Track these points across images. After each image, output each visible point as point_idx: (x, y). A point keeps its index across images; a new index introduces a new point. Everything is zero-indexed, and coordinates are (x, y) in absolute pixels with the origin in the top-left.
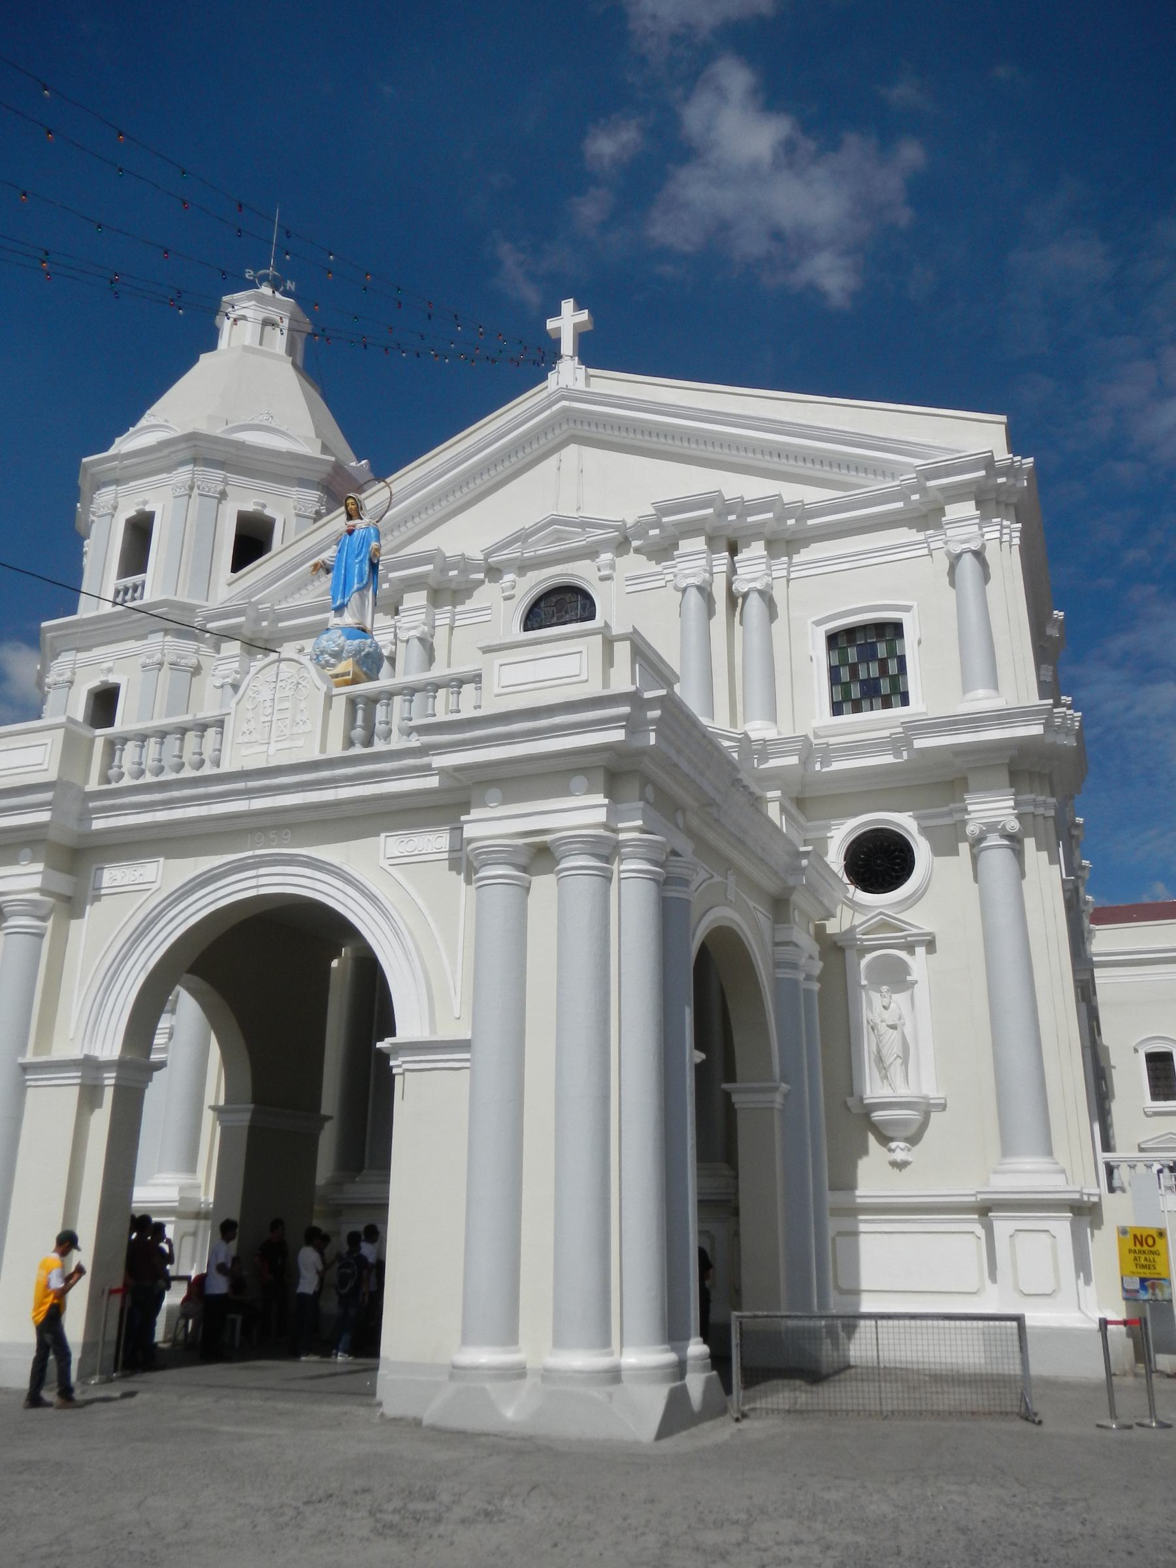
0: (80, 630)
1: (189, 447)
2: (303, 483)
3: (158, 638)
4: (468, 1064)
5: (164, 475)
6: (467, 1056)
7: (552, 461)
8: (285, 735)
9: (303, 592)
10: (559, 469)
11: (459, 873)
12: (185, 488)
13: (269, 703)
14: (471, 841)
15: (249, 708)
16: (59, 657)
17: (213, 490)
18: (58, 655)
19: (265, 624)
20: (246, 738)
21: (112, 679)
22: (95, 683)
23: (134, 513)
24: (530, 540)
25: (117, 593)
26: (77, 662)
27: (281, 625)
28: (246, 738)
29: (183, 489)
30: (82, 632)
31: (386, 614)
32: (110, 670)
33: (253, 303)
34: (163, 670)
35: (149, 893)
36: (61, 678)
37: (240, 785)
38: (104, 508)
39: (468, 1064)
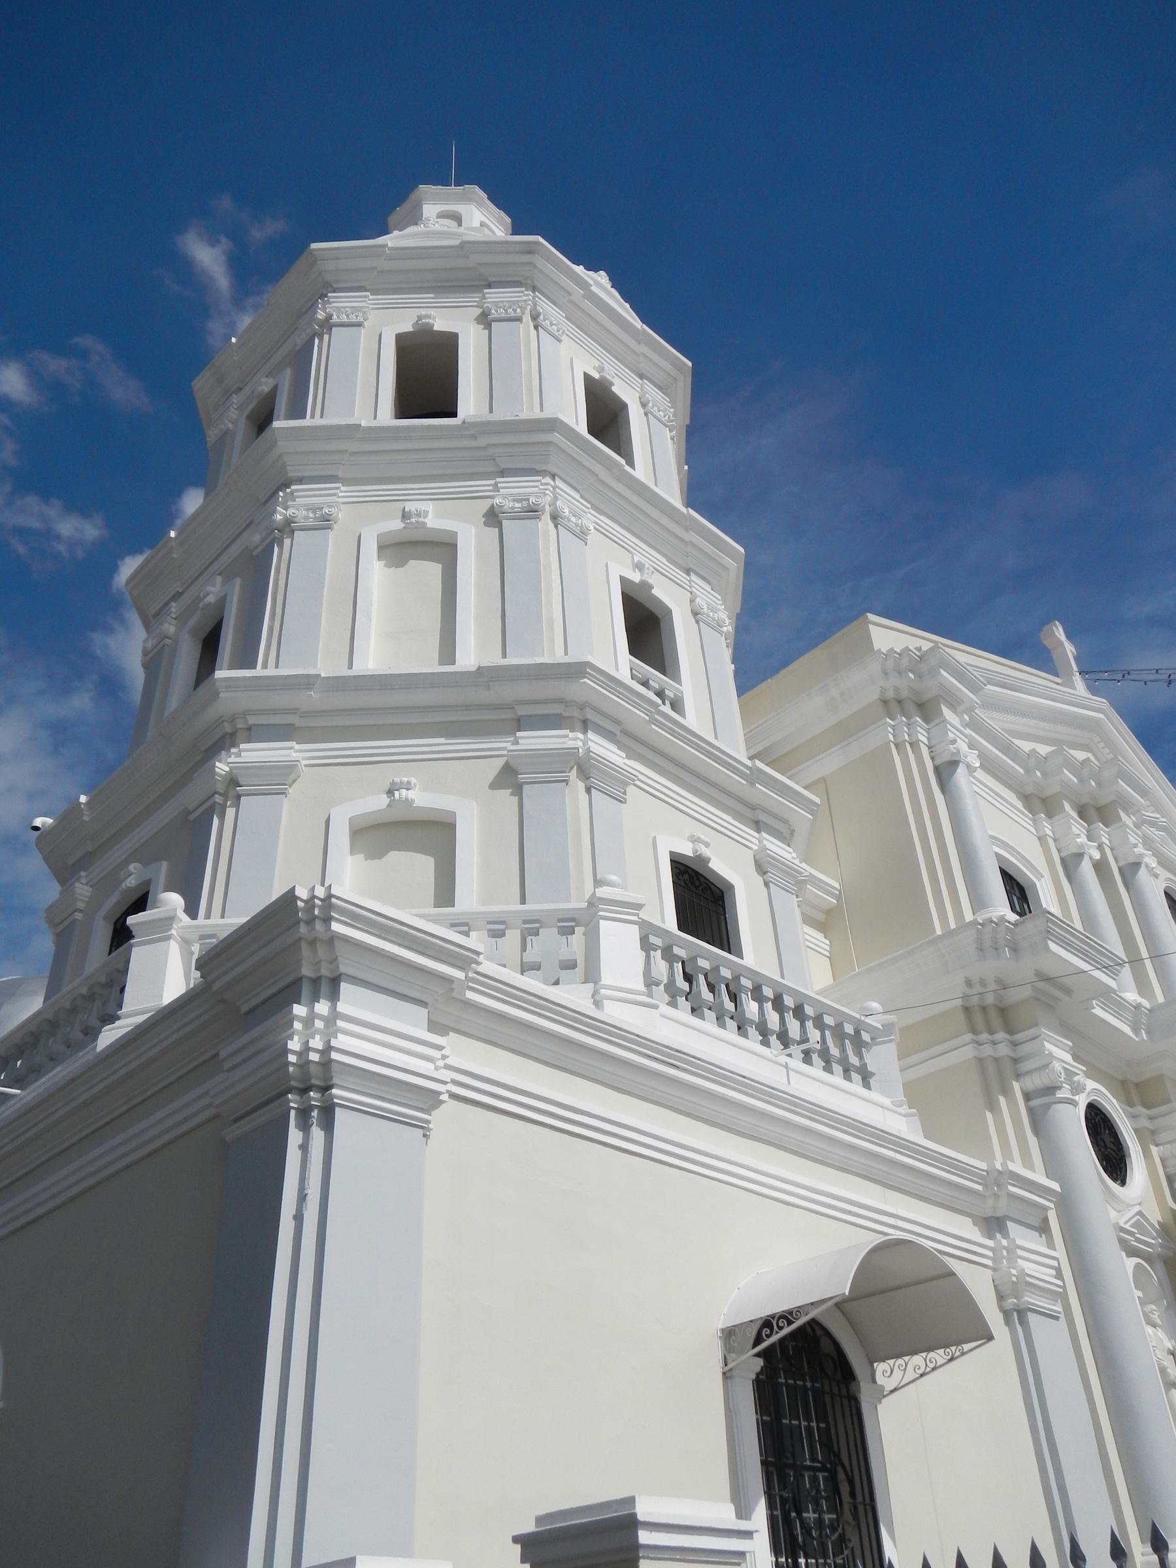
38: (551, 324)
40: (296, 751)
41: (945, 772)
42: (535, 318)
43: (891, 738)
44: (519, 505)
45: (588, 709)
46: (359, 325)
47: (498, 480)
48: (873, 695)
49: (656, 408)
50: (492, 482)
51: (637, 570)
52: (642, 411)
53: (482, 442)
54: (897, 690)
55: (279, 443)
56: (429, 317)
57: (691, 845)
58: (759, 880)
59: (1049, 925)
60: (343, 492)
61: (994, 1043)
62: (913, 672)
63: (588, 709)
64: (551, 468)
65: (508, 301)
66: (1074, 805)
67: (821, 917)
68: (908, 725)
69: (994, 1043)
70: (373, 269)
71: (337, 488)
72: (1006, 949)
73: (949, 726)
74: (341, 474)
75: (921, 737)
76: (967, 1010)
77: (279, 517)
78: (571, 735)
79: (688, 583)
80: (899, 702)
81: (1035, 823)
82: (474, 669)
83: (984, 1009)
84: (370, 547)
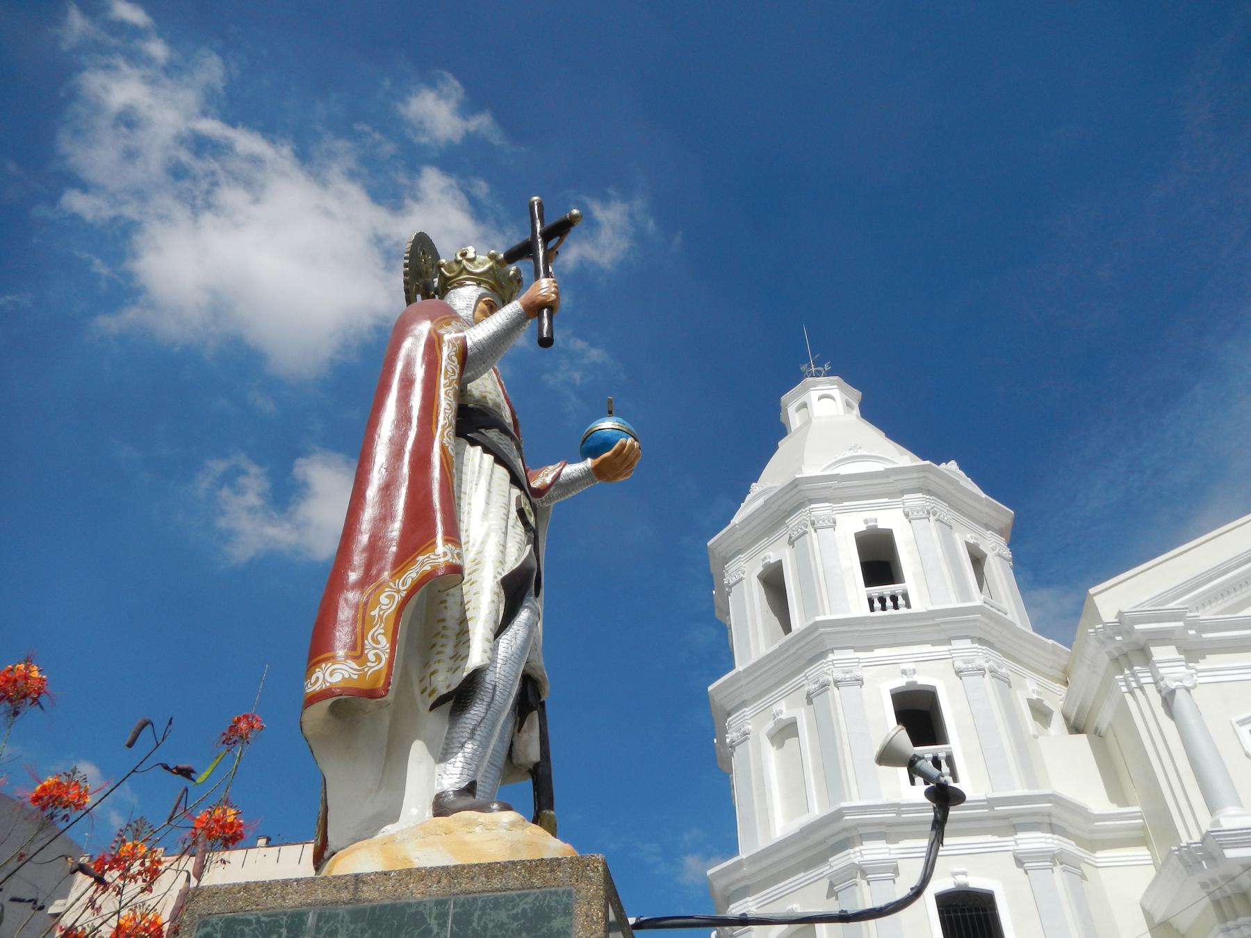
0: (861, 628)
1: (918, 478)
2: (987, 527)
3: (967, 643)
5: (886, 500)
9: (1208, 608)
12: (924, 512)
16: (830, 655)
17: (946, 518)
18: (832, 650)
19: (1192, 632)
21: (923, 680)
22: (900, 682)
23: (865, 529)
25: (871, 602)
26: (861, 661)
27: (1204, 636)
29: (921, 513)
30: (862, 631)
32: (914, 672)
33: (836, 387)
34: (985, 676)
36: (848, 676)
38: (824, 521)
40: (750, 902)
41: (1168, 699)
42: (813, 524)
43: (1124, 689)
44: (816, 686)
45: (859, 828)
46: (741, 579)
47: (806, 671)
48: (1106, 659)
49: (915, 513)
50: (803, 674)
51: (904, 676)
52: (907, 520)
53: (792, 651)
54: (1117, 649)
55: (715, 698)
56: (765, 558)
57: (953, 879)
58: (1022, 870)
59: (1217, 839)
60: (747, 711)
61: (1238, 927)
62: (1119, 634)
63: (859, 828)
64: (828, 647)
65: (797, 524)
67: (1140, 833)
68: (1133, 674)
69: (1238, 927)
70: (737, 539)
71: (745, 711)
72: (1203, 862)
73: (1158, 665)
74: (746, 697)
75: (1143, 680)
76: (1217, 903)
77: (728, 740)
78: (851, 851)
79: (948, 653)
80: (1125, 655)
82: (798, 830)
83: (1229, 897)
84: (766, 742)
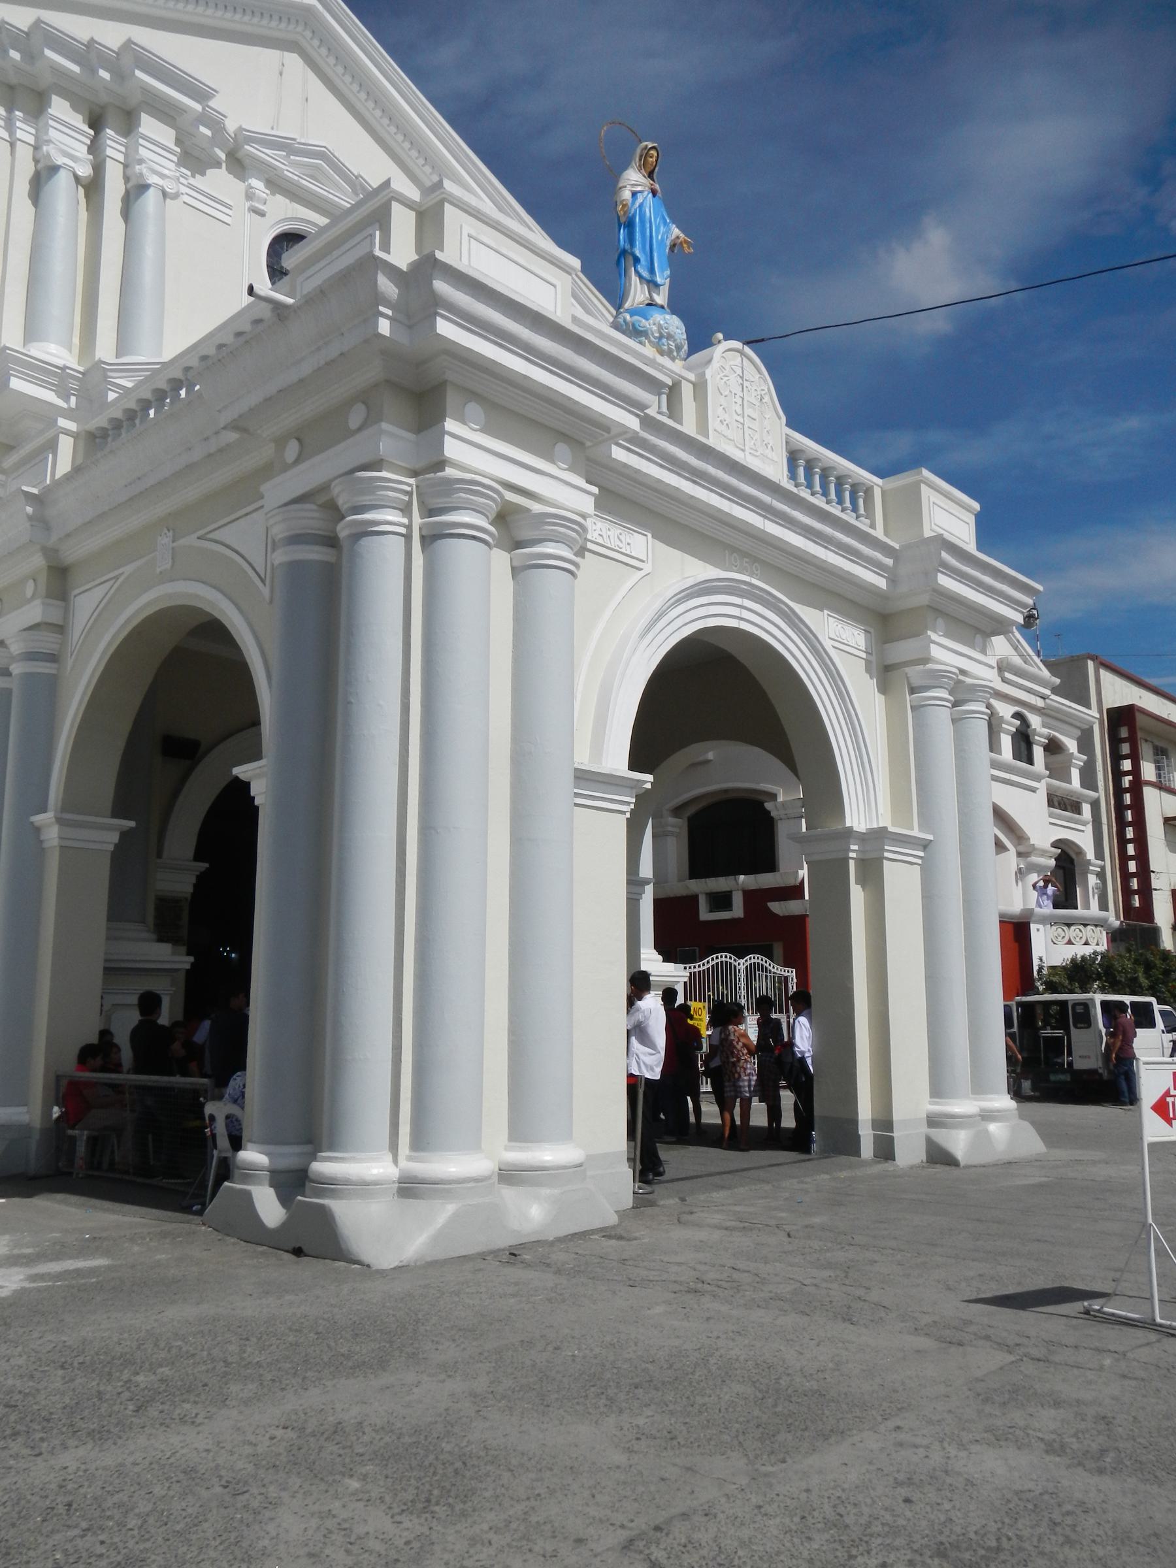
4: (920, 861)
6: (921, 854)
7: (271, 56)
8: (756, 451)
10: (281, 74)
11: (871, 678)
13: (739, 401)
14: (926, 660)
15: (722, 392)
20: (722, 428)
24: (292, 157)
28: (722, 428)
31: (75, 107)
35: (640, 574)
37: (766, 498)
39: (920, 861)
66: (76, 103)
81: (10, 126)
